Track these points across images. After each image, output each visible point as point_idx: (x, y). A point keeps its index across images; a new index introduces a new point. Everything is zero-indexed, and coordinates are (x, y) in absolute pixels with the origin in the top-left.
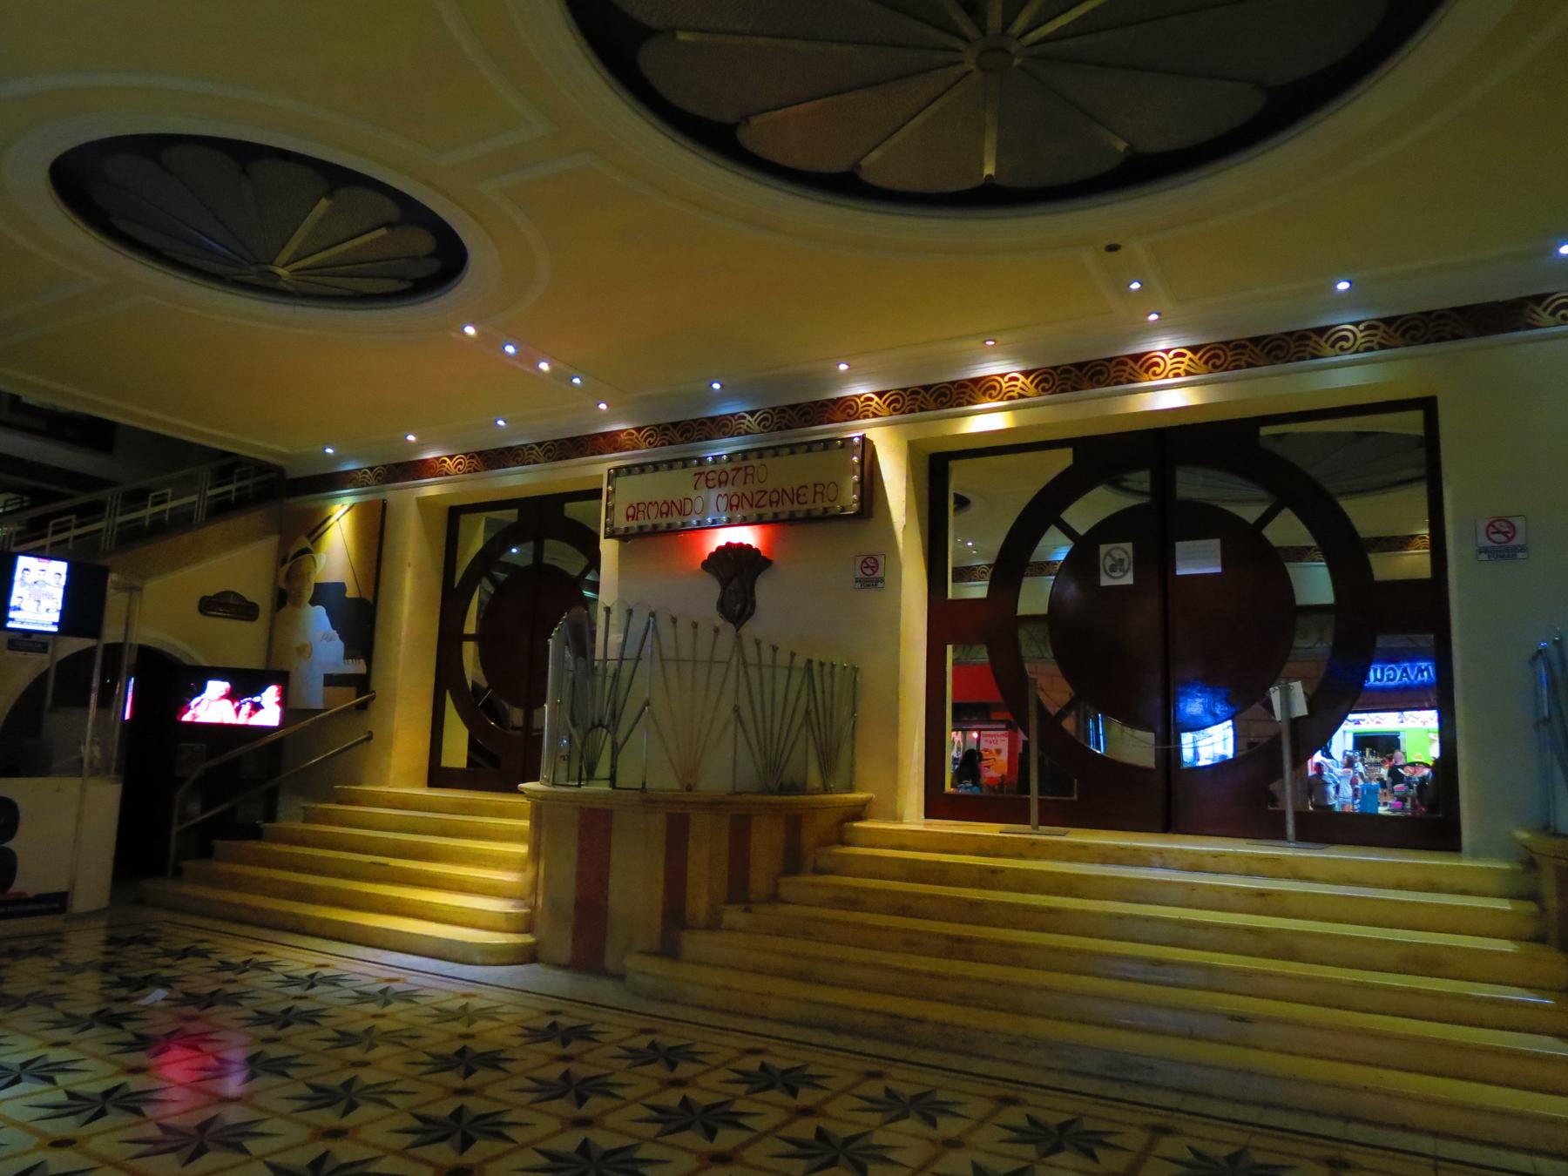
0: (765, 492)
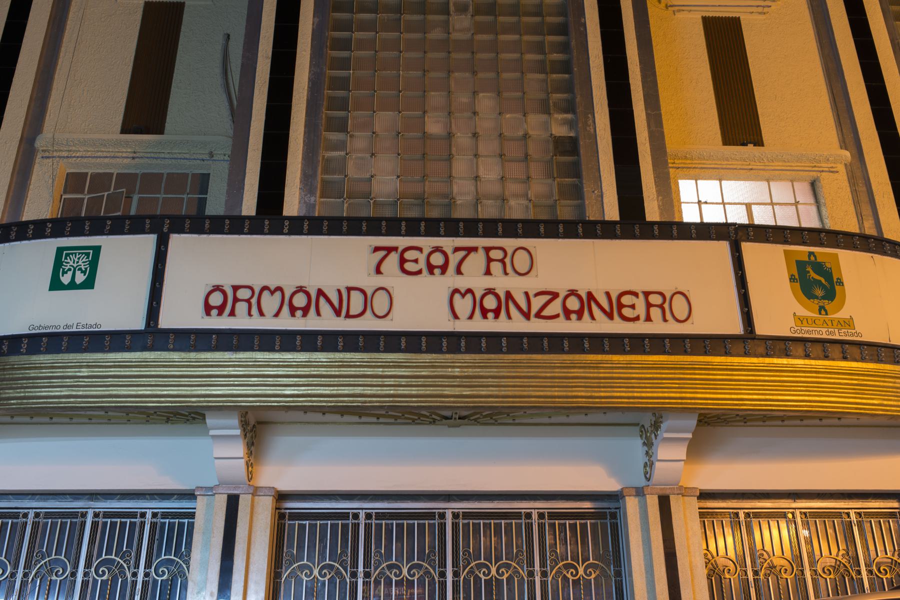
0: (555, 295)
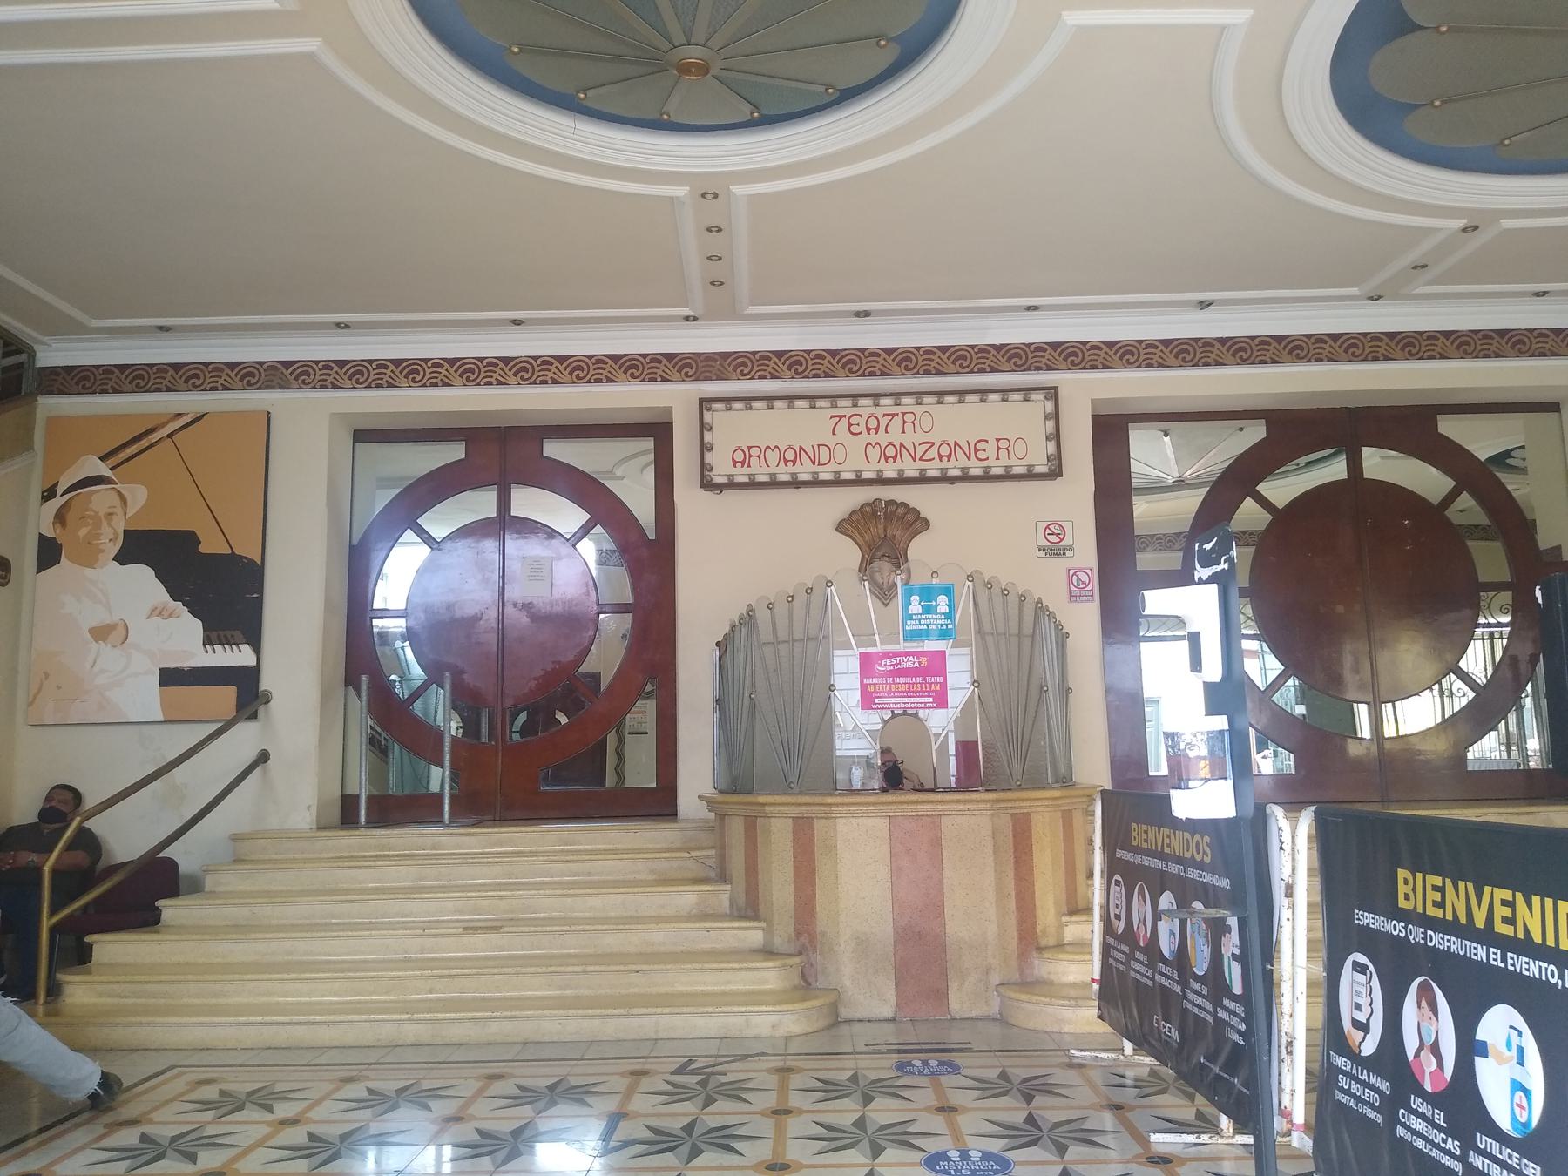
0: (933, 444)
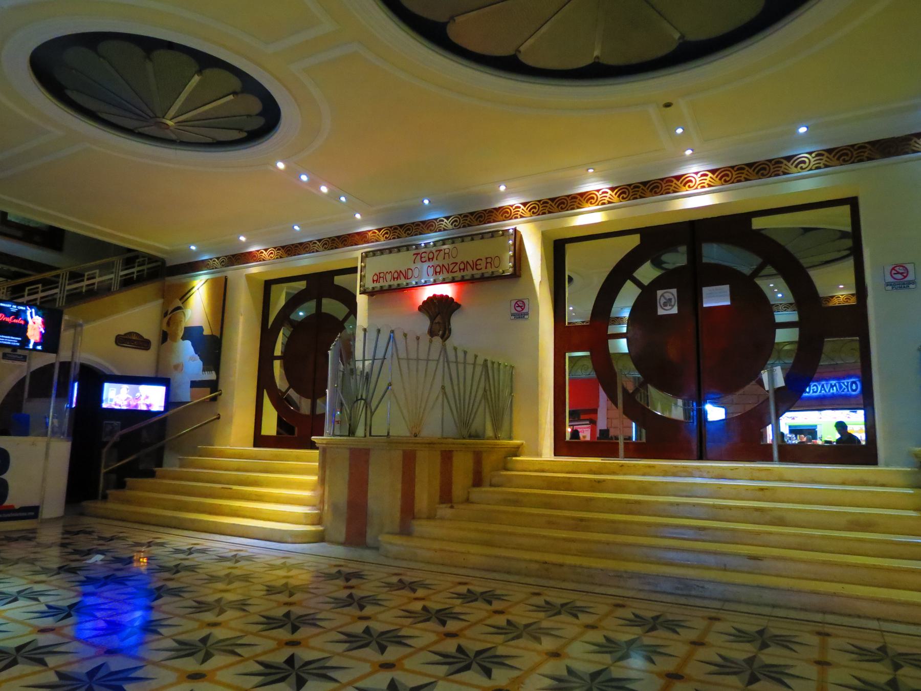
0: (457, 263)
